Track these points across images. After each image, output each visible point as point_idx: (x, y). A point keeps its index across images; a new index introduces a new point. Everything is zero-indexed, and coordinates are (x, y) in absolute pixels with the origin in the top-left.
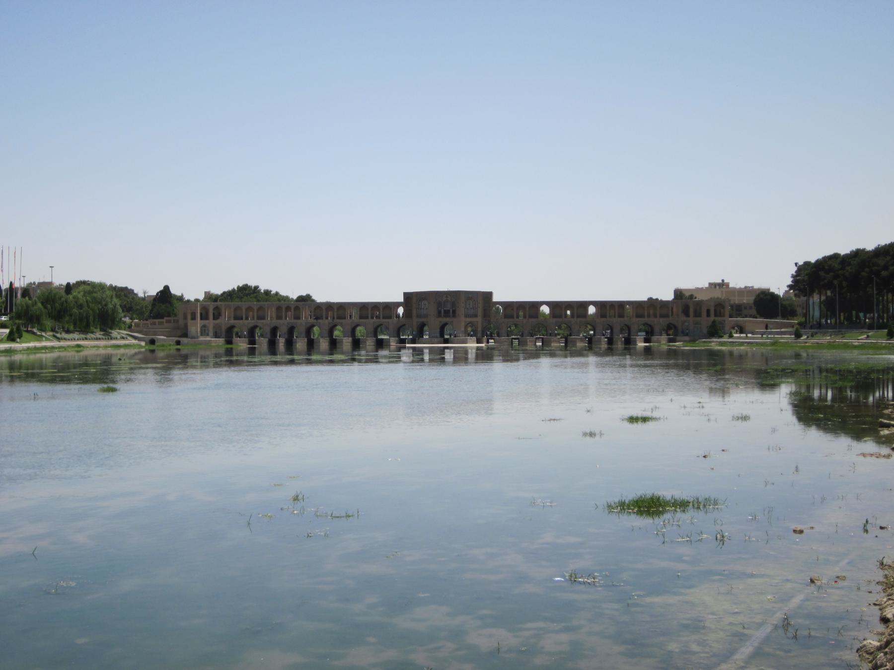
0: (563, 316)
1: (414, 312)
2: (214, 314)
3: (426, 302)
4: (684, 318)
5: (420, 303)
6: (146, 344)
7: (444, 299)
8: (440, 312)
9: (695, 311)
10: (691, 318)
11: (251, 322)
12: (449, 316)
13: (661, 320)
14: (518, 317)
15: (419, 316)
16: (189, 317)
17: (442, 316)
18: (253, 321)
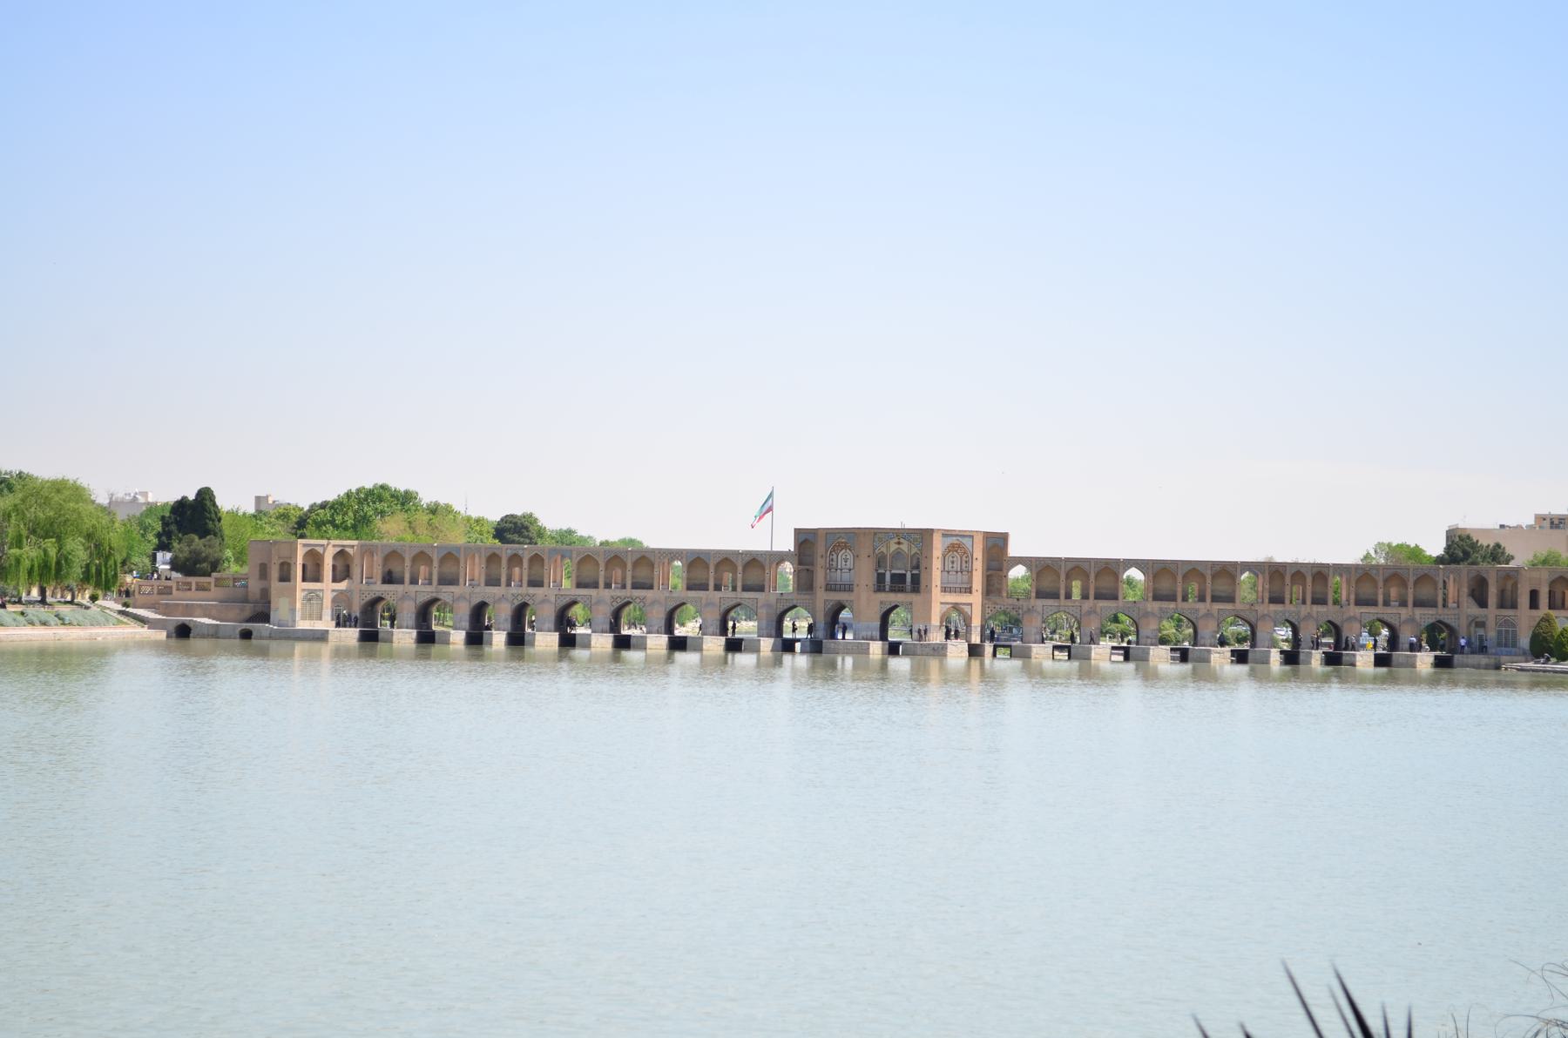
0: (1179, 598)
1: (820, 579)
2: (334, 567)
3: (850, 555)
4: (1474, 610)
5: (835, 557)
6: (168, 637)
7: (893, 547)
8: (880, 578)
9: (1502, 593)
10: (1492, 613)
11: (423, 592)
12: (902, 590)
13: (1419, 612)
14: (1068, 596)
15: (830, 588)
16: (275, 573)
17: (887, 588)
18: (429, 588)
